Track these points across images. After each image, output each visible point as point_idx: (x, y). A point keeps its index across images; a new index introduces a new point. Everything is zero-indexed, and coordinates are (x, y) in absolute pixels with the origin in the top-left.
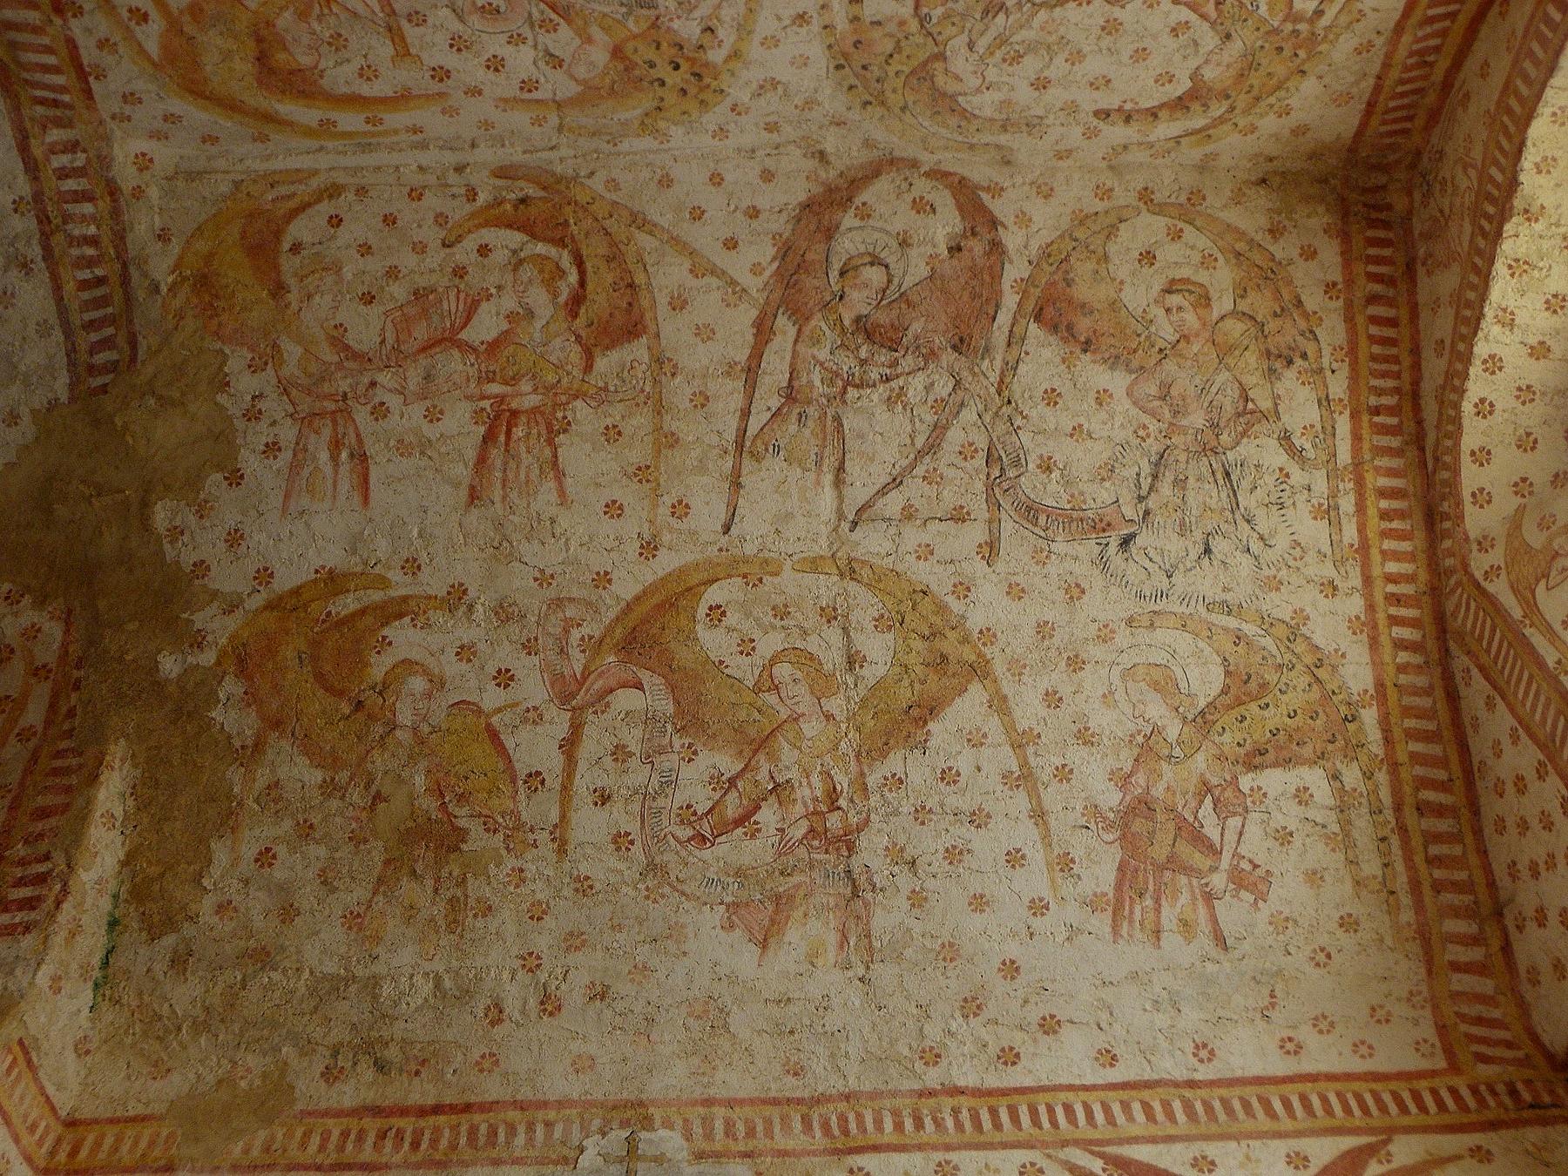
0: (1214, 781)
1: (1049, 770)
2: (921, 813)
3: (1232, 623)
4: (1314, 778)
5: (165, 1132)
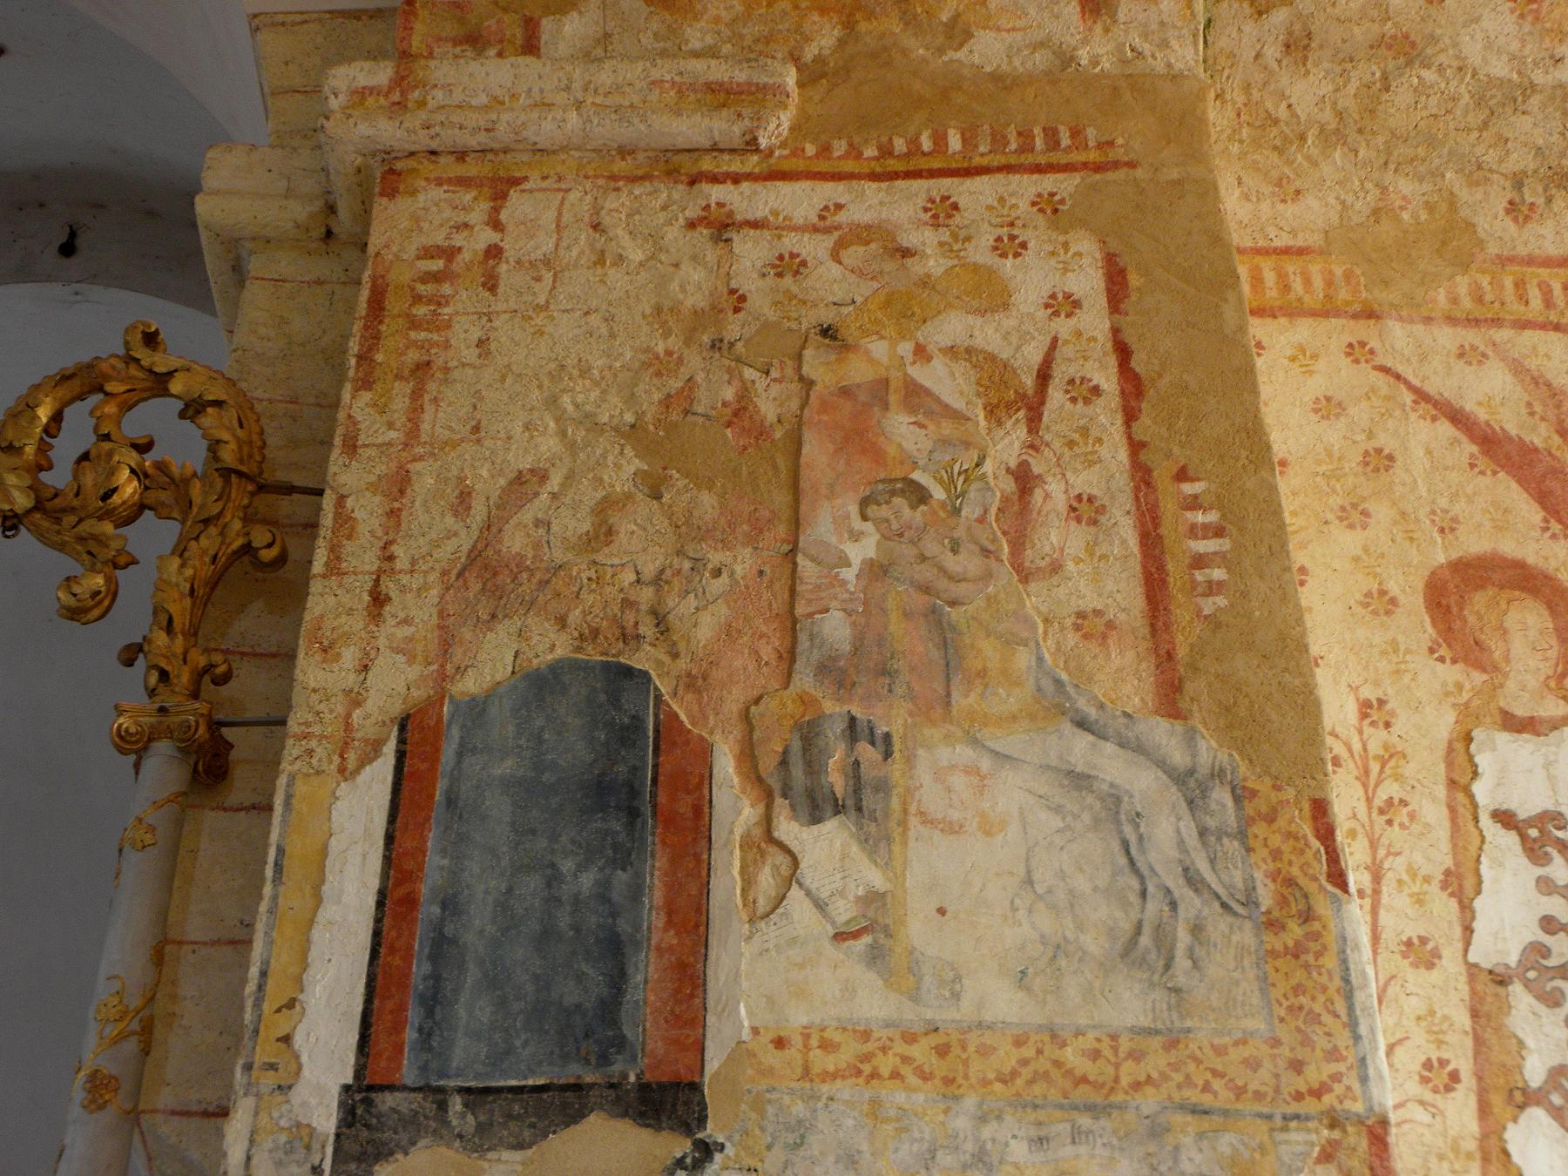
5: (1339, 271)
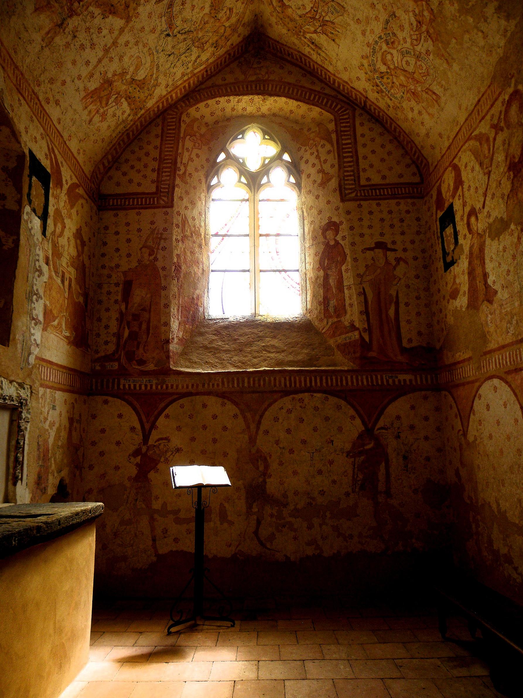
0: (121, 94)
1: (111, 56)
2: (88, 29)
3: (155, 72)
4: (128, 111)
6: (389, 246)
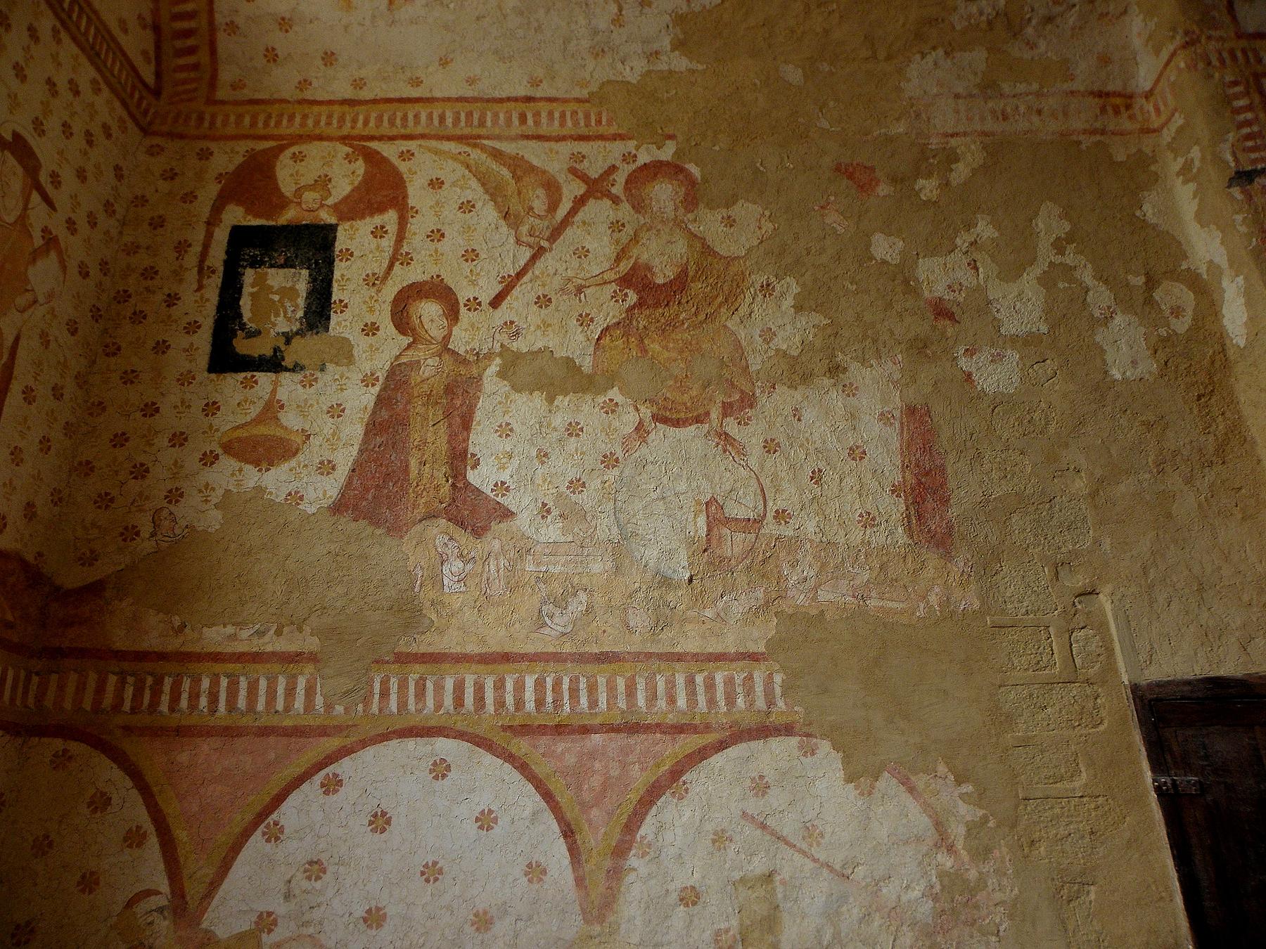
6: (44, 178)
